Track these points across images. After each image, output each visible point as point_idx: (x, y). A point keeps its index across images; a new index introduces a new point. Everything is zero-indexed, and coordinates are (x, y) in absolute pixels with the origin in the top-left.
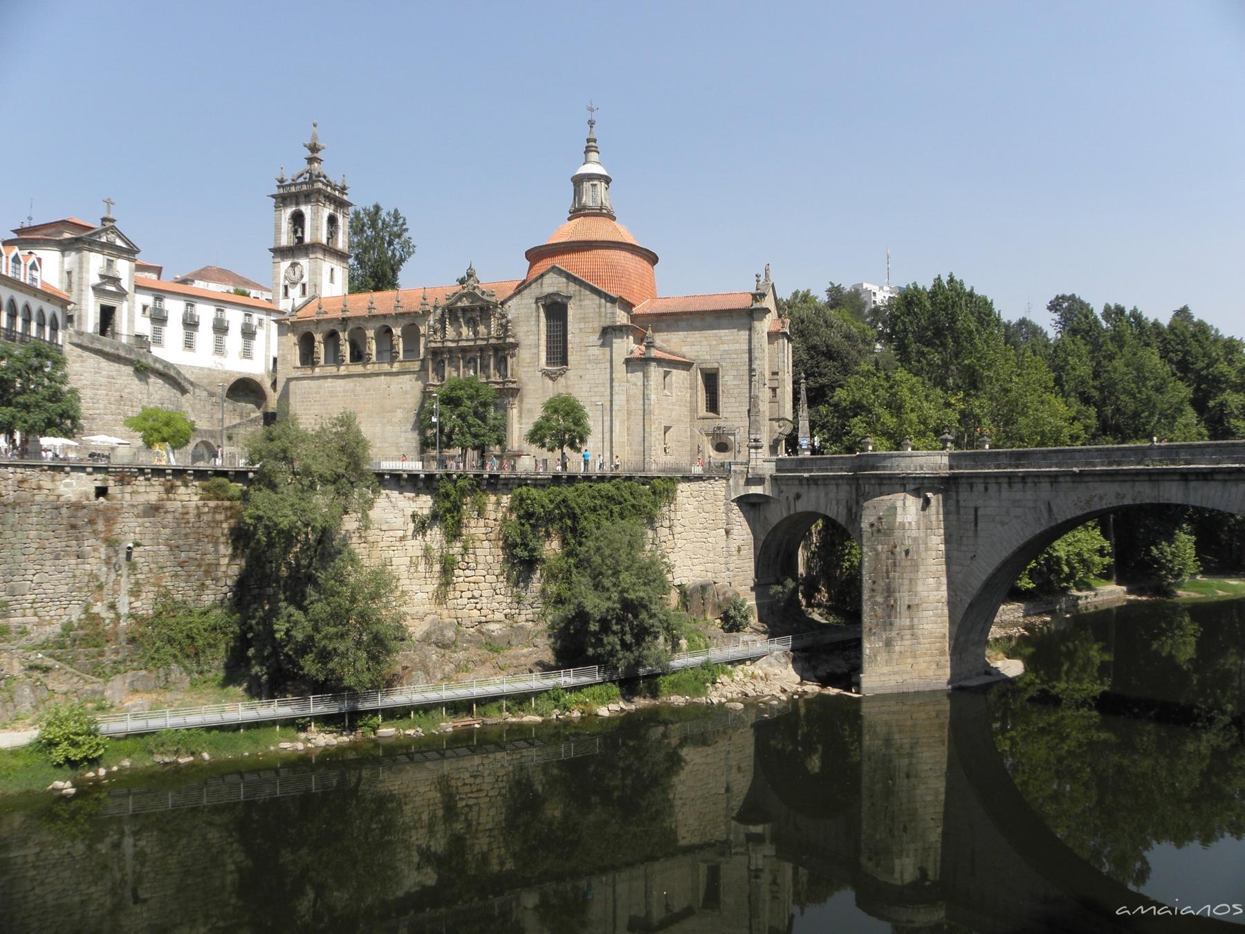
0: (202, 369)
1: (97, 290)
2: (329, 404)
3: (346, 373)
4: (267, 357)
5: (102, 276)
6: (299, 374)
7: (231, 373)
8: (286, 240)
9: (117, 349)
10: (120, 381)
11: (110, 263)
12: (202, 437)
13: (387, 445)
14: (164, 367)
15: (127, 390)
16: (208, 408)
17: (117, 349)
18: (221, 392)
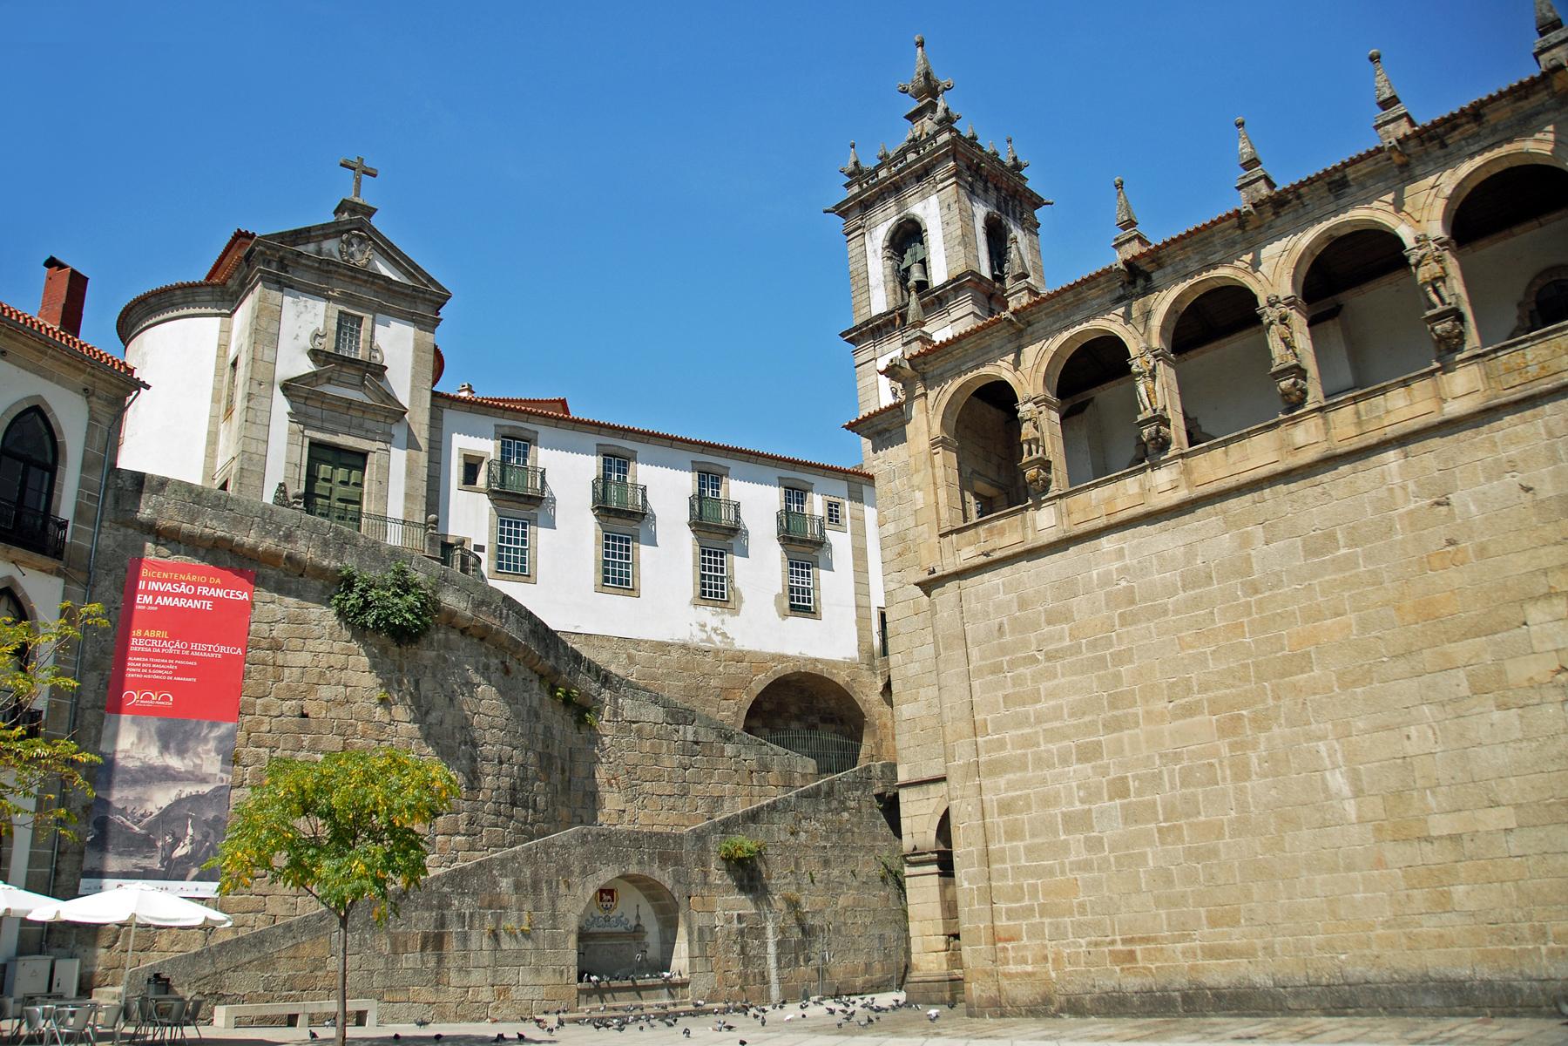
0: (662, 647)
1: (287, 387)
2: (1119, 658)
3: (1182, 494)
4: (862, 609)
5: (315, 354)
6: (968, 554)
7: (759, 661)
8: (880, 302)
9: (288, 537)
10: (304, 658)
11: (348, 326)
12: (621, 859)
13: (1493, 819)
14: (478, 605)
15: (325, 692)
16: (670, 762)
17: (288, 537)
18: (732, 712)
